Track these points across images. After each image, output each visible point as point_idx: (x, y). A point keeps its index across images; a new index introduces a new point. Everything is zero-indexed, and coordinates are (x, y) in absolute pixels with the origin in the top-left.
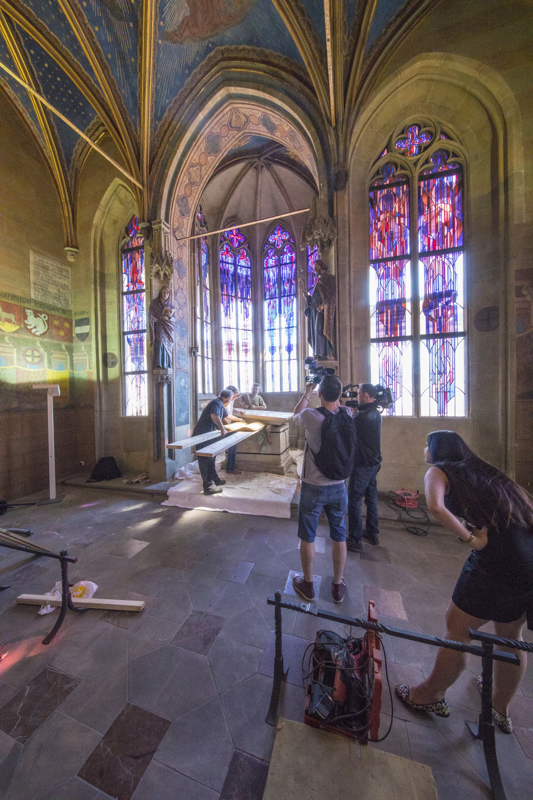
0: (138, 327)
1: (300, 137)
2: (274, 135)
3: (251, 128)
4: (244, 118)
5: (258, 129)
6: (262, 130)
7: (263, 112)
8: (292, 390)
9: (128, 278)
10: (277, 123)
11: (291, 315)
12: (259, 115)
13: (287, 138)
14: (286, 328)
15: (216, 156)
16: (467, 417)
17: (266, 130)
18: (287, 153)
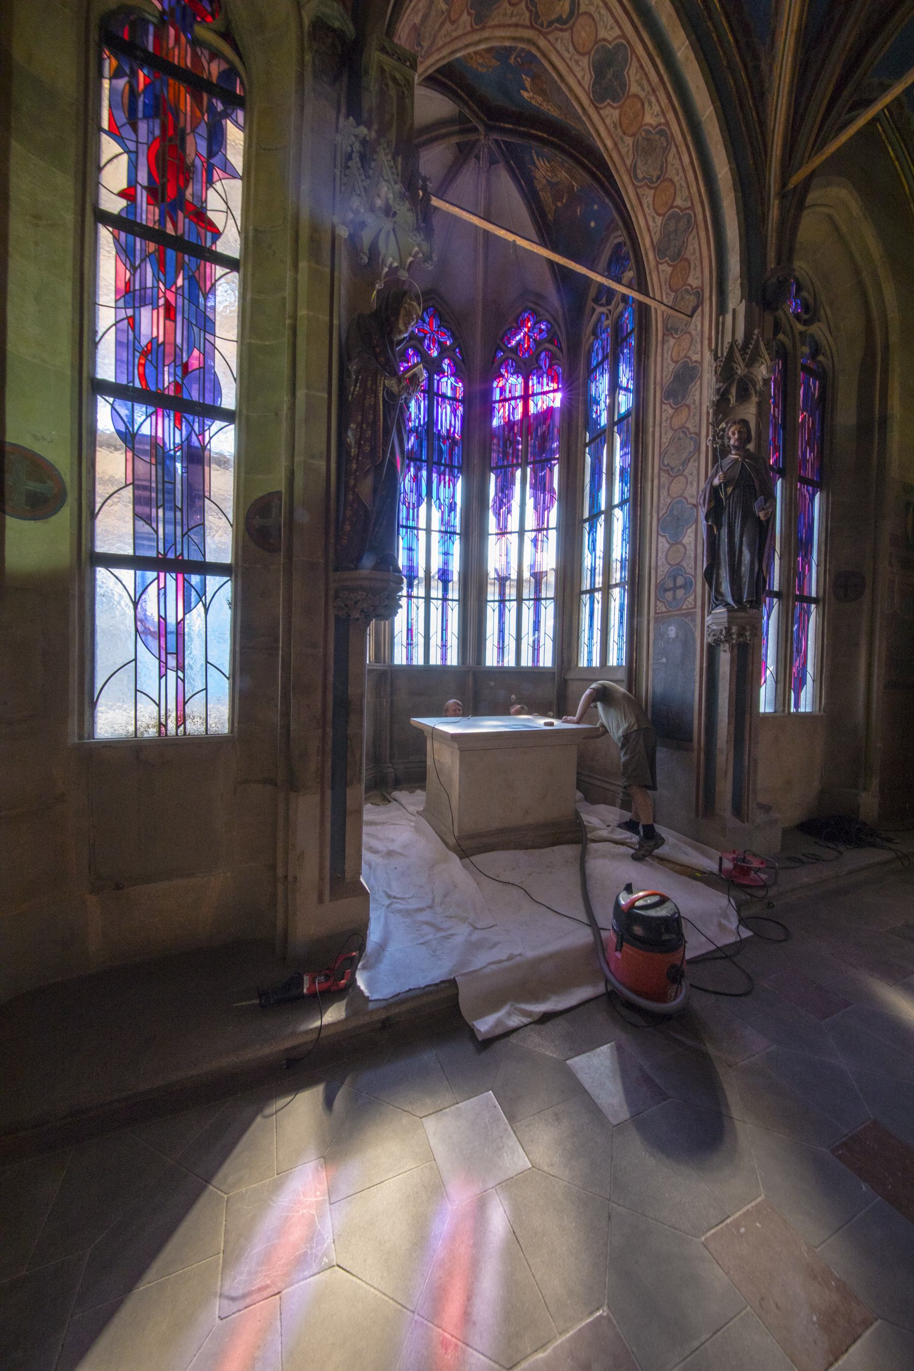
0: (178, 387)
1: (680, 162)
2: (596, 108)
3: (559, 46)
4: (567, 7)
5: (572, 64)
6: (579, 75)
7: (624, 36)
8: (449, 663)
9: (133, 167)
10: (634, 89)
11: (452, 507)
12: (608, 33)
13: (629, 141)
14: (440, 531)
15: (473, 31)
16: (817, 712)
17: (587, 81)
18: (533, 168)
